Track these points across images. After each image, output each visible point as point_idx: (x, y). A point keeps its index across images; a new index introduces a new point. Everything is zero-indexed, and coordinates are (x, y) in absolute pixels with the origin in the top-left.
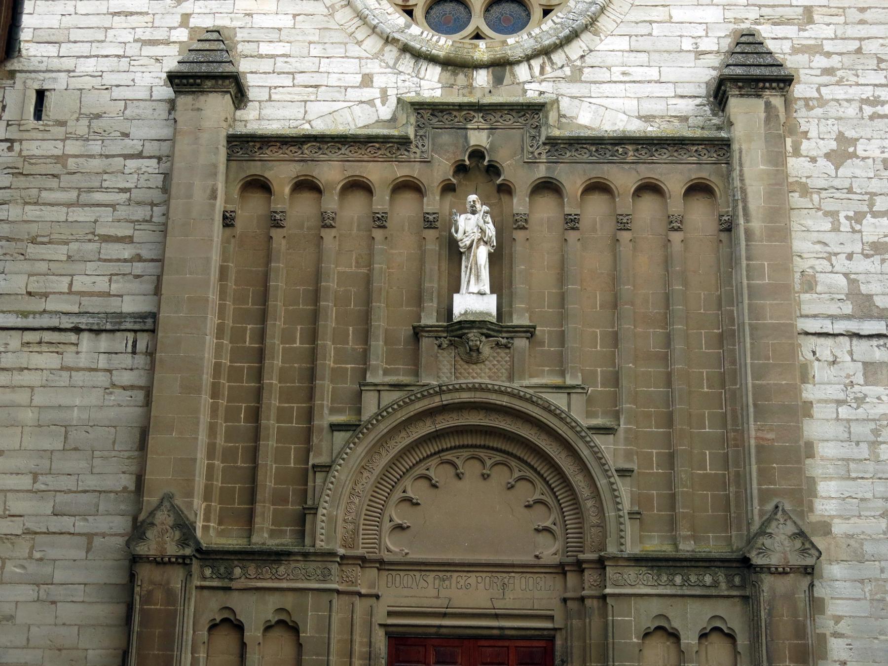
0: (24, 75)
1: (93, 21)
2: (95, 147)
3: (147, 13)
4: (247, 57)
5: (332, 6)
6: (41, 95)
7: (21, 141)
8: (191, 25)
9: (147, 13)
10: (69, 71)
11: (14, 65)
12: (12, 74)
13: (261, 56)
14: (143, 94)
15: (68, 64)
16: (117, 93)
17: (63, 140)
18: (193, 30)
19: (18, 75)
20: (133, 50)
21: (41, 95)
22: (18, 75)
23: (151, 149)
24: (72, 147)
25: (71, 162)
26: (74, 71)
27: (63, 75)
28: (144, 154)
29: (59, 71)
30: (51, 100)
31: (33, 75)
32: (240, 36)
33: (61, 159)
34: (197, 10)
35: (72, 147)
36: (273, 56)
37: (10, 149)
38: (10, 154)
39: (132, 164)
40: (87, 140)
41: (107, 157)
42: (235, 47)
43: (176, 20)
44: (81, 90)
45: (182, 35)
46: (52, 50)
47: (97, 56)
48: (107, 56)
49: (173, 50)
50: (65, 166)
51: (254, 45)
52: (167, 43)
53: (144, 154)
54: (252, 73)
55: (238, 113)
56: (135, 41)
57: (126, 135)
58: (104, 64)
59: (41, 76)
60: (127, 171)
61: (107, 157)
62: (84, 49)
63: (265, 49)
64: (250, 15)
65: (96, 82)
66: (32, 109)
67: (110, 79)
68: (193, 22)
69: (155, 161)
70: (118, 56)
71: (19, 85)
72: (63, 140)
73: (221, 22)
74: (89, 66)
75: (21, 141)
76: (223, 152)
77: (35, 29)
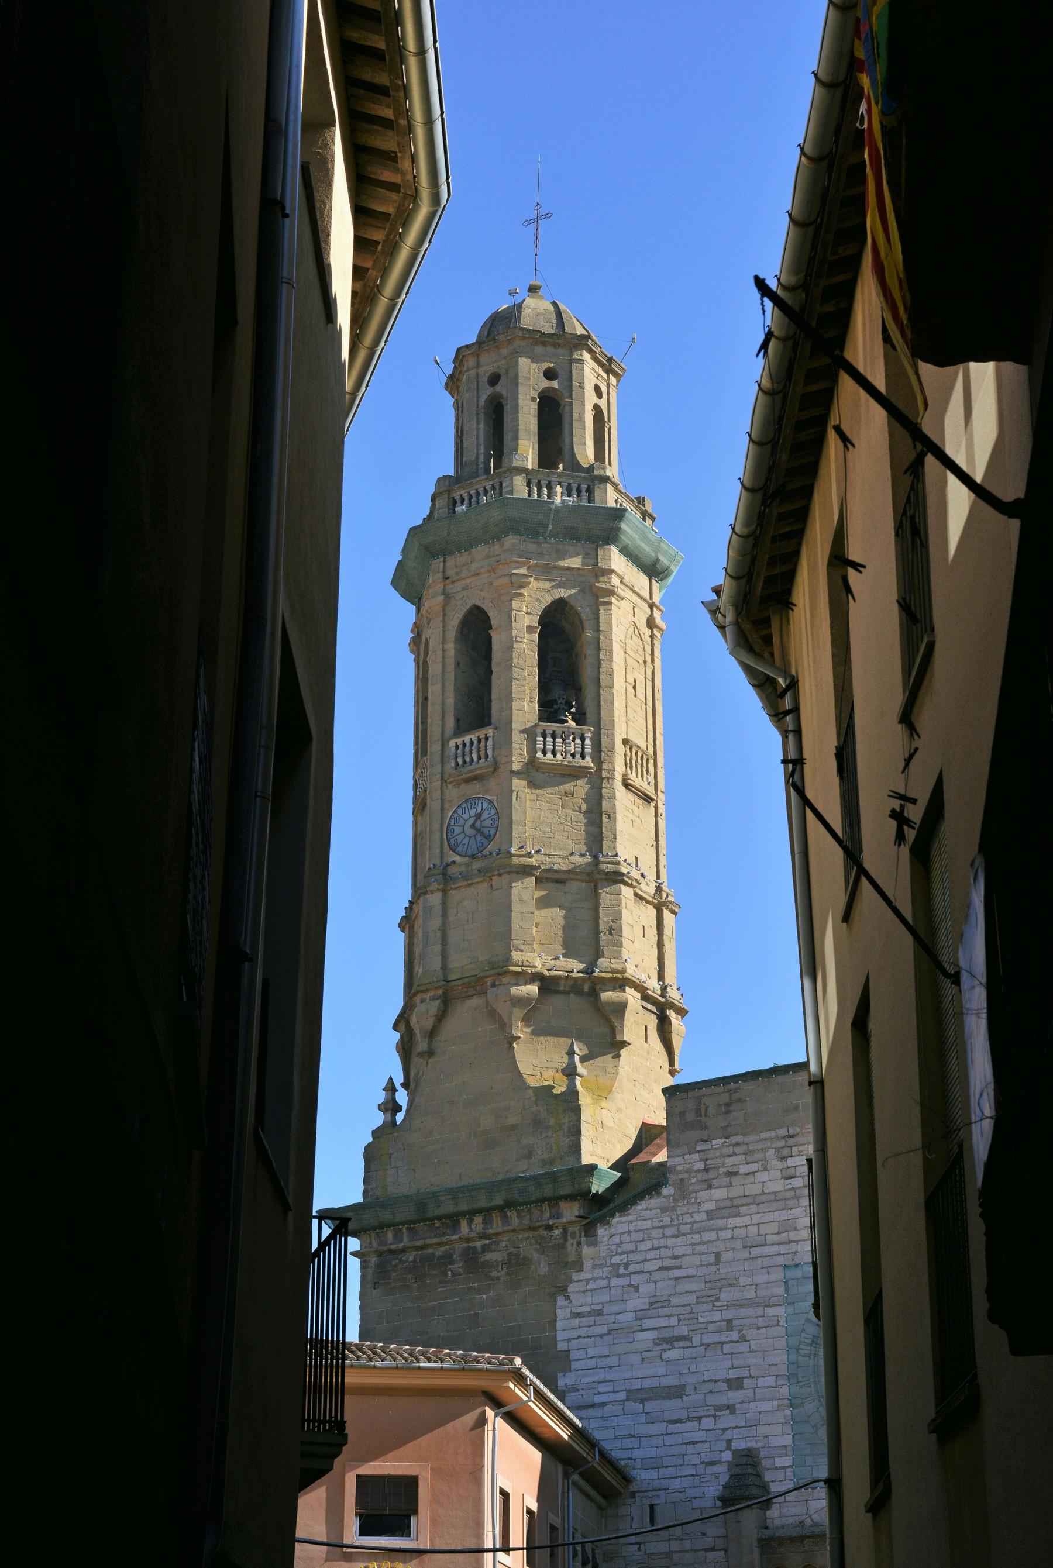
0: (640, 1494)
1: (675, 1450)
2: (688, 1544)
3: (706, 1441)
4: (768, 1469)
5: (815, 1425)
6: (652, 1507)
7: (644, 1543)
8: (733, 1448)
9: (706, 1441)
10: (666, 1489)
11: (633, 1487)
12: (633, 1494)
13: (777, 1468)
14: (709, 1503)
15: (664, 1483)
16: (696, 1503)
17: (669, 1541)
18: (735, 1452)
19: (637, 1494)
20: (701, 1469)
21: (652, 1506)
22: (637, 1494)
23: (720, 1544)
24: (675, 1546)
25: (675, 1556)
26: (668, 1489)
27: (662, 1492)
28: (717, 1548)
29: (660, 1490)
30: (658, 1510)
31: (645, 1494)
32: (763, 1453)
33: (669, 1554)
34: (735, 1437)
35: (675, 1546)
36: (783, 1468)
37: (639, 1549)
38: (640, 1553)
39: (710, 1555)
40: (682, 1539)
41: (696, 1551)
42: (760, 1463)
43: (724, 1445)
44: (674, 1502)
45: (727, 1456)
46: (651, 1474)
47: (680, 1476)
48: (686, 1476)
49: (722, 1469)
50: (672, 1560)
51: (771, 1461)
52: (720, 1462)
53: (717, 1548)
54: (772, 1481)
55: (768, 1513)
56: (702, 1463)
57: (704, 1534)
58: (686, 1482)
59: (650, 1494)
60: (708, 1561)
61: (696, 1551)
62: (672, 1471)
63: (779, 1462)
64: (767, 1437)
65: (681, 1496)
66: (648, 1519)
67: (692, 1493)
68: (735, 1445)
69: (723, 1552)
70: (693, 1475)
71: (638, 1502)
72: (669, 1541)
73: (751, 1444)
74: (676, 1484)
75: (644, 1543)
76: (757, 1552)
77: (642, 1459)
